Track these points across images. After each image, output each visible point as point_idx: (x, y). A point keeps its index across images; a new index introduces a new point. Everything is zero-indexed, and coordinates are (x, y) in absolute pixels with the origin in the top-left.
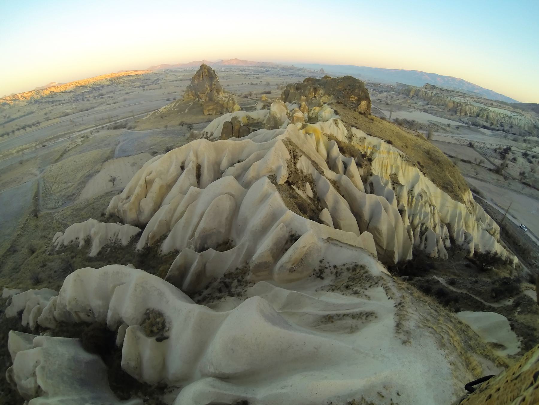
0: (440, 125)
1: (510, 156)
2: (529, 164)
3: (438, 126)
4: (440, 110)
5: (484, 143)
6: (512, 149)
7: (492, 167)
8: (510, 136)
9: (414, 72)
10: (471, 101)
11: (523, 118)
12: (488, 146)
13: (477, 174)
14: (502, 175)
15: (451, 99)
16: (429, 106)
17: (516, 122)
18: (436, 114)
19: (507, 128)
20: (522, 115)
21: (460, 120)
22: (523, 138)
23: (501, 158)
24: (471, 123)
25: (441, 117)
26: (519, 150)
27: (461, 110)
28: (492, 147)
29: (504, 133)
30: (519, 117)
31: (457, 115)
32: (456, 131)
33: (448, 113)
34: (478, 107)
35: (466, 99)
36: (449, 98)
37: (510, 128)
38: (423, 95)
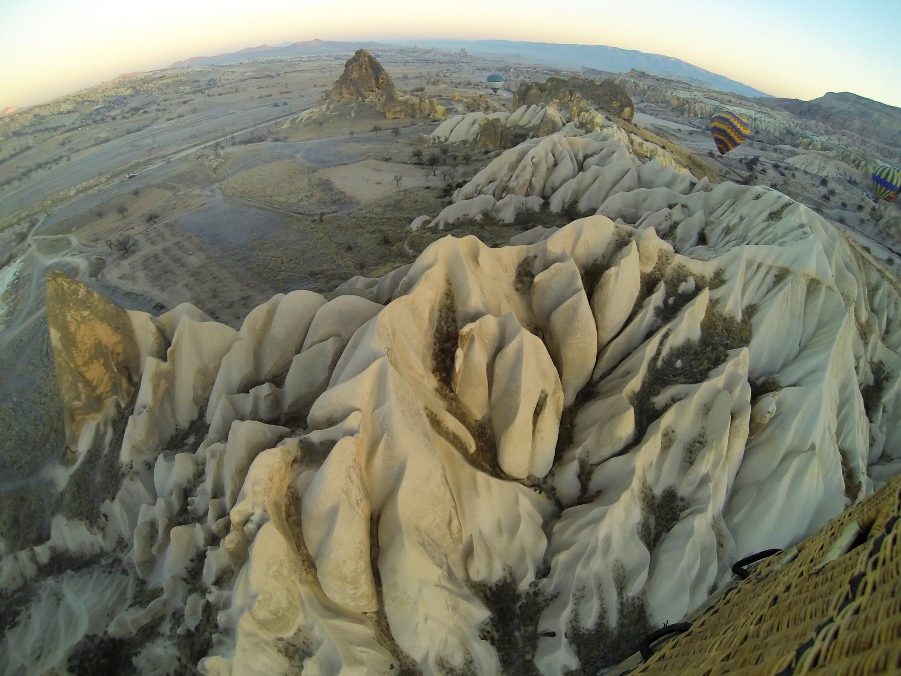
0: (667, 130)
1: (759, 167)
2: (780, 176)
3: (666, 132)
7: (740, 179)
8: (756, 144)
11: (772, 121)
15: (672, 93)
16: (645, 104)
17: (762, 126)
18: (656, 116)
20: (771, 116)
21: (690, 123)
22: (772, 147)
23: (748, 169)
24: (704, 127)
25: (665, 119)
26: (770, 161)
28: (735, 157)
30: (768, 120)
32: (688, 137)
33: (672, 113)
35: (692, 94)
36: (669, 92)
37: (755, 133)
38: (632, 89)
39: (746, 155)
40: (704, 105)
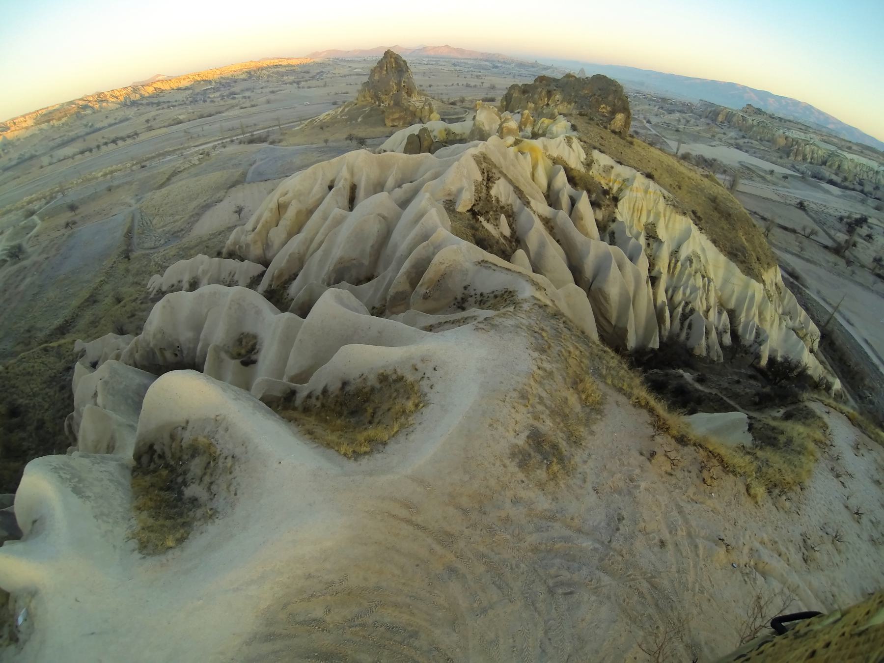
0: (756, 171)
1: (864, 230)
3: (753, 172)
4: (763, 148)
5: (825, 206)
6: (870, 220)
7: (829, 243)
8: (871, 202)
9: (732, 86)
10: (816, 139)
12: (831, 211)
13: (802, 249)
14: (843, 257)
16: (746, 140)
18: (754, 154)
19: (868, 188)
21: (793, 167)
23: (848, 231)
24: (810, 173)
25: (762, 158)
27: (797, 151)
28: (836, 214)
29: (862, 196)
31: (790, 158)
32: (782, 182)
34: (828, 150)
35: (808, 136)
36: (781, 131)
38: (739, 123)
39: (851, 213)
40: (816, 148)
